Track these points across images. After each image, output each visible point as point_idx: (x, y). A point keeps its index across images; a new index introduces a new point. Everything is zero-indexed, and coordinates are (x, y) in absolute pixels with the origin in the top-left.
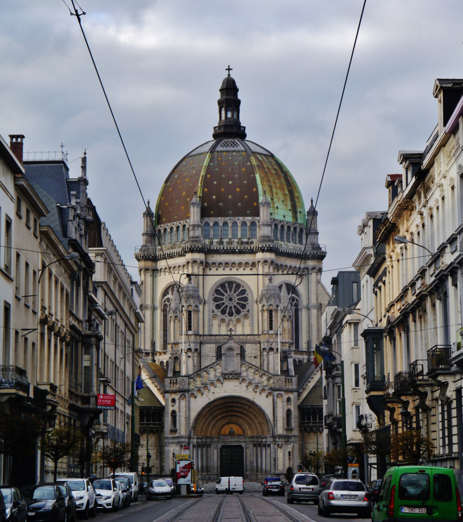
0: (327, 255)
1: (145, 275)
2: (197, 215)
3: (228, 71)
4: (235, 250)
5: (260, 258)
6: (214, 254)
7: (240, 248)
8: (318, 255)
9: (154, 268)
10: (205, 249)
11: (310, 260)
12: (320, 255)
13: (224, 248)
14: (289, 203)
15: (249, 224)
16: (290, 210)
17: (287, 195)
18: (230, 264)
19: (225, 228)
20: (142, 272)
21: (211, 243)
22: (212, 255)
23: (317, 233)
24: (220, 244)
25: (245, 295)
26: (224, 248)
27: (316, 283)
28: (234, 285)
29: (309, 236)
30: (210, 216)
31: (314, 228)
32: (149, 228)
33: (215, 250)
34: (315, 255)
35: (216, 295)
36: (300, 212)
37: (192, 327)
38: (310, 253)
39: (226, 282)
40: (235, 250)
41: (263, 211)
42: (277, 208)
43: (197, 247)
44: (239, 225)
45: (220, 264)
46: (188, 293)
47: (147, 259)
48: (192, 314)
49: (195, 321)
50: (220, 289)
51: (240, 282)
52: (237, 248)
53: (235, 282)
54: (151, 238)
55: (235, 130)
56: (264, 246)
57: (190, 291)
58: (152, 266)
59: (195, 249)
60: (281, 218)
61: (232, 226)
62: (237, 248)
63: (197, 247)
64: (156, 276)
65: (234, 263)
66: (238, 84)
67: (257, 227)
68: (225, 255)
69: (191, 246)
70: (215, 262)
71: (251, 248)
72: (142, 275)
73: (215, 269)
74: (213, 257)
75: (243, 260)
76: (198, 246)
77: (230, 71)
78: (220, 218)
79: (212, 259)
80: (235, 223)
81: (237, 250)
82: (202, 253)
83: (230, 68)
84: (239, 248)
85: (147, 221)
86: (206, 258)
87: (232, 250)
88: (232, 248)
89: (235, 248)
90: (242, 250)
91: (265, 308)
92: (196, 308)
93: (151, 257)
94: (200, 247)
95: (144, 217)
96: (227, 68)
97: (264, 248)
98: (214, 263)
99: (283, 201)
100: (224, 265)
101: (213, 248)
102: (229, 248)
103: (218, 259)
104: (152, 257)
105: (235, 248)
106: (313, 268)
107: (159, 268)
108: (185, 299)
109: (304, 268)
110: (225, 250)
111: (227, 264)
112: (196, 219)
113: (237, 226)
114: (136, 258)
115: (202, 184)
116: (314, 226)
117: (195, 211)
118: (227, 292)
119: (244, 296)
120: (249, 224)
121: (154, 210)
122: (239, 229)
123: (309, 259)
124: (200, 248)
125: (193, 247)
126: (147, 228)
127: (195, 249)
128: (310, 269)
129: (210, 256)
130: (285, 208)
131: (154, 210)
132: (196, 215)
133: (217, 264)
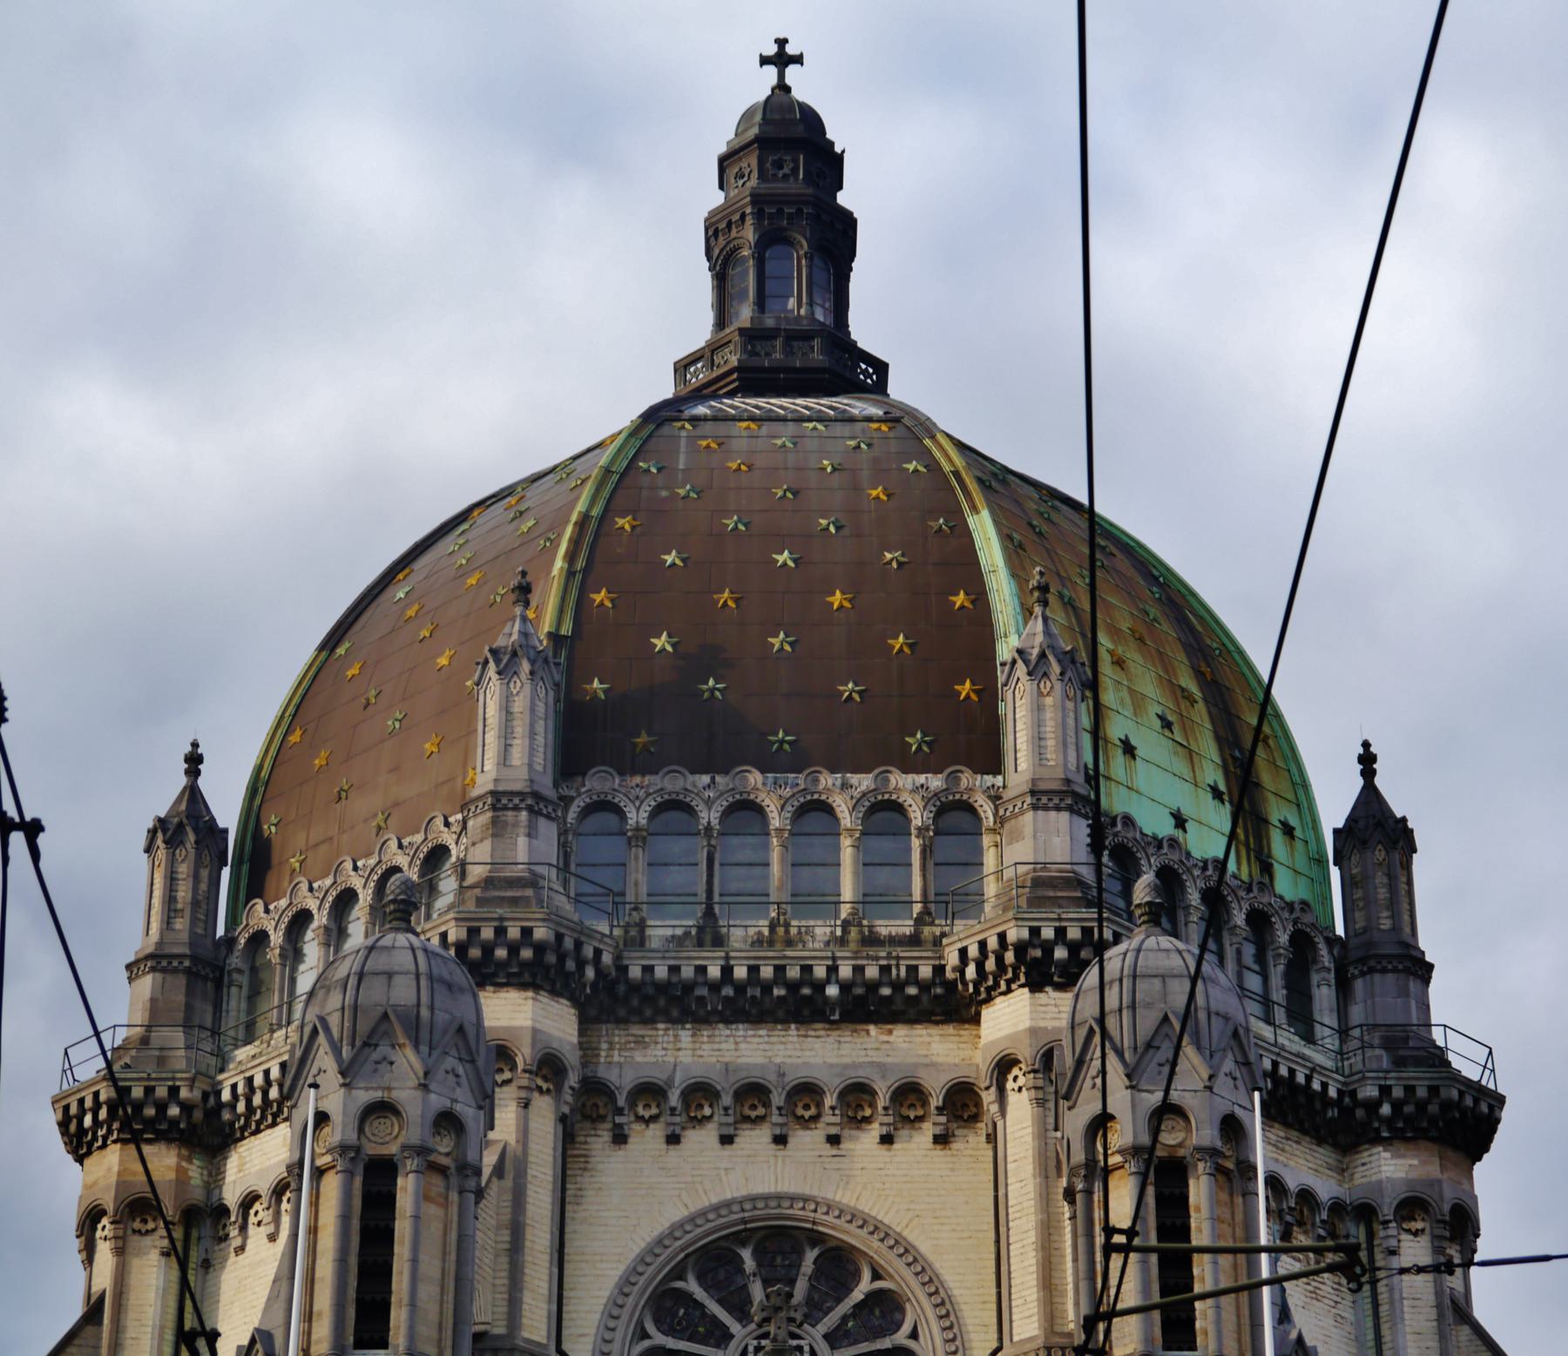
0: (1506, 1114)
1: (120, 1252)
2: (532, 734)
3: (772, 71)
4: (820, 987)
5: (1013, 1037)
6: (650, 1022)
7: (859, 970)
8: (1447, 1106)
9: (197, 1196)
10: (581, 964)
11: (1386, 1142)
12: (1458, 1105)
13: (727, 970)
14: (1208, 748)
15: (918, 815)
16: (1217, 794)
17: (1193, 702)
18: (777, 1099)
19: (740, 848)
20: (105, 1228)
21: (635, 938)
22: (637, 1030)
23: (1422, 970)
24: (700, 944)
25: (901, 1337)
26: (727, 970)
27: (1440, 1318)
28: (811, 1255)
29: (1359, 985)
30: (631, 764)
31: (1396, 928)
32: (181, 924)
33: (663, 988)
34: (1422, 1106)
35: (659, 1339)
36: (1288, 831)
37: (398, 1317)
38: (1385, 1091)
39: (741, 1238)
40: (820, 987)
41: (1039, 708)
42: (1129, 750)
43: (514, 933)
44: (846, 818)
45: (700, 1092)
46: (374, 994)
47: (150, 1124)
48: (406, 1188)
49: (431, 1266)
50: (692, 1286)
51: (854, 1237)
52: (832, 969)
53: (816, 1238)
54: (190, 991)
55: (817, 355)
56: (1048, 933)
57: (390, 975)
58: (182, 1180)
59: (501, 953)
60: (1165, 828)
62: (832, 969)
63: (514, 933)
64: (206, 1265)
65: (807, 1091)
66: (837, 133)
67: (987, 840)
68: (741, 1030)
69: (473, 932)
70: (659, 1076)
71: (939, 970)
72: (105, 1253)
73: (657, 1132)
74: (640, 1042)
75: (883, 1068)
76: (527, 932)
77: (792, 72)
78: (706, 779)
79: (639, 1057)
80: (815, 810)
81: (832, 991)
82: (555, 993)
83: (791, 49)
84: (845, 971)
85: (171, 880)
86: (587, 1048)
87: (793, 987)
88: (793, 973)
89: (820, 972)
90: (873, 987)
91: (1121, 1135)
92: (444, 1145)
93: (174, 1111)
94: (540, 933)
95: (148, 850)
96: (772, 50)
97: (1048, 948)
98: (650, 1091)
99: (1167, 725)
100: (727, 1100)
101: (648, 969)
102: (767, 972)
103: (685, 1057)
104: (186, 1107)
105: (820, 972)
106: (1412, 1206)
107: (231, 1196)
108: (336, 1050)
109: (1337, 1207)
110: (740, 988)
111: (753, 1093)
112: (518, 756)
113: (833, 830)
114: (63, 1125)
115: (580, 564)
116: (1395, 916)
117: (520, 705)
118: (742, 1315)
119: (885, 1343)
120: (918, 815)
121: (227, 811)
123: (1377, 1140)
124: (540, 948)
125: (487, 933)
126: (168, 923)
127: (501, 953)
128: (1387, 1211)
129: (619, 1036)
130: (1182, 767)
131: (227, 811)
132: (520, 729)
133: (674, 1099)
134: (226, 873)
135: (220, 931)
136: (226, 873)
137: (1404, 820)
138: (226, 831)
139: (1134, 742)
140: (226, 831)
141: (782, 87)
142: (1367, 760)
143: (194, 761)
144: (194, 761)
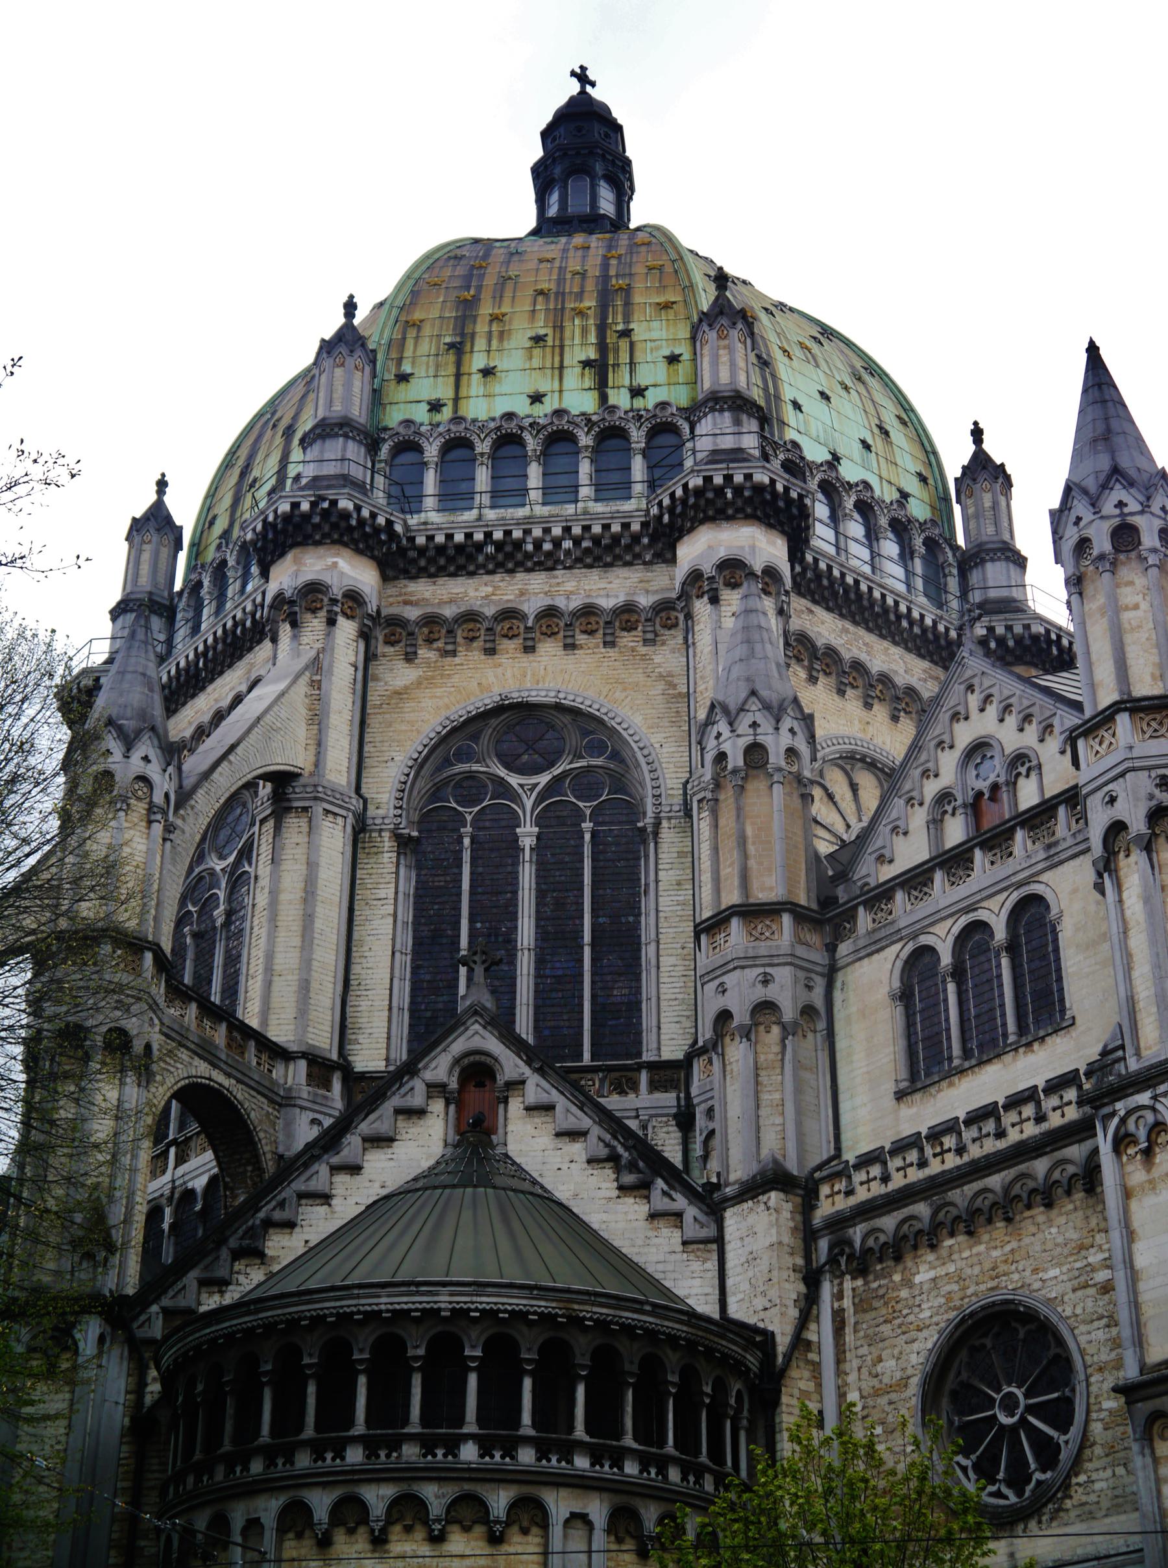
42: (797, 406)
56: (718, 480)
61: (544, 453)
66: (618, 114)
110: (499, 546)
122: (585, 468)
134: (182, 557)
135: (178, 586)
136: (182, 557)
137: (1002, 465)
138: (181, 527)
139: (800, 402)
140: (181, 527)
141: (583, 92)
142: (977, 434)
143: (162, 485)
144: (162, 485)
